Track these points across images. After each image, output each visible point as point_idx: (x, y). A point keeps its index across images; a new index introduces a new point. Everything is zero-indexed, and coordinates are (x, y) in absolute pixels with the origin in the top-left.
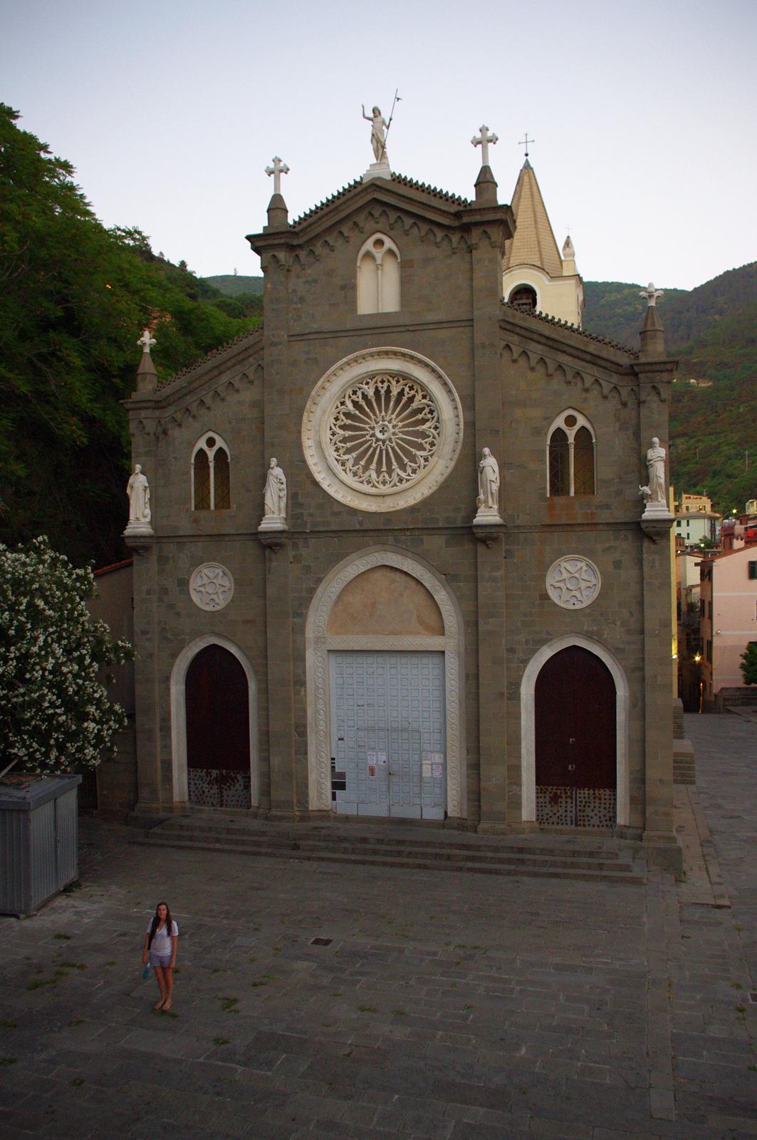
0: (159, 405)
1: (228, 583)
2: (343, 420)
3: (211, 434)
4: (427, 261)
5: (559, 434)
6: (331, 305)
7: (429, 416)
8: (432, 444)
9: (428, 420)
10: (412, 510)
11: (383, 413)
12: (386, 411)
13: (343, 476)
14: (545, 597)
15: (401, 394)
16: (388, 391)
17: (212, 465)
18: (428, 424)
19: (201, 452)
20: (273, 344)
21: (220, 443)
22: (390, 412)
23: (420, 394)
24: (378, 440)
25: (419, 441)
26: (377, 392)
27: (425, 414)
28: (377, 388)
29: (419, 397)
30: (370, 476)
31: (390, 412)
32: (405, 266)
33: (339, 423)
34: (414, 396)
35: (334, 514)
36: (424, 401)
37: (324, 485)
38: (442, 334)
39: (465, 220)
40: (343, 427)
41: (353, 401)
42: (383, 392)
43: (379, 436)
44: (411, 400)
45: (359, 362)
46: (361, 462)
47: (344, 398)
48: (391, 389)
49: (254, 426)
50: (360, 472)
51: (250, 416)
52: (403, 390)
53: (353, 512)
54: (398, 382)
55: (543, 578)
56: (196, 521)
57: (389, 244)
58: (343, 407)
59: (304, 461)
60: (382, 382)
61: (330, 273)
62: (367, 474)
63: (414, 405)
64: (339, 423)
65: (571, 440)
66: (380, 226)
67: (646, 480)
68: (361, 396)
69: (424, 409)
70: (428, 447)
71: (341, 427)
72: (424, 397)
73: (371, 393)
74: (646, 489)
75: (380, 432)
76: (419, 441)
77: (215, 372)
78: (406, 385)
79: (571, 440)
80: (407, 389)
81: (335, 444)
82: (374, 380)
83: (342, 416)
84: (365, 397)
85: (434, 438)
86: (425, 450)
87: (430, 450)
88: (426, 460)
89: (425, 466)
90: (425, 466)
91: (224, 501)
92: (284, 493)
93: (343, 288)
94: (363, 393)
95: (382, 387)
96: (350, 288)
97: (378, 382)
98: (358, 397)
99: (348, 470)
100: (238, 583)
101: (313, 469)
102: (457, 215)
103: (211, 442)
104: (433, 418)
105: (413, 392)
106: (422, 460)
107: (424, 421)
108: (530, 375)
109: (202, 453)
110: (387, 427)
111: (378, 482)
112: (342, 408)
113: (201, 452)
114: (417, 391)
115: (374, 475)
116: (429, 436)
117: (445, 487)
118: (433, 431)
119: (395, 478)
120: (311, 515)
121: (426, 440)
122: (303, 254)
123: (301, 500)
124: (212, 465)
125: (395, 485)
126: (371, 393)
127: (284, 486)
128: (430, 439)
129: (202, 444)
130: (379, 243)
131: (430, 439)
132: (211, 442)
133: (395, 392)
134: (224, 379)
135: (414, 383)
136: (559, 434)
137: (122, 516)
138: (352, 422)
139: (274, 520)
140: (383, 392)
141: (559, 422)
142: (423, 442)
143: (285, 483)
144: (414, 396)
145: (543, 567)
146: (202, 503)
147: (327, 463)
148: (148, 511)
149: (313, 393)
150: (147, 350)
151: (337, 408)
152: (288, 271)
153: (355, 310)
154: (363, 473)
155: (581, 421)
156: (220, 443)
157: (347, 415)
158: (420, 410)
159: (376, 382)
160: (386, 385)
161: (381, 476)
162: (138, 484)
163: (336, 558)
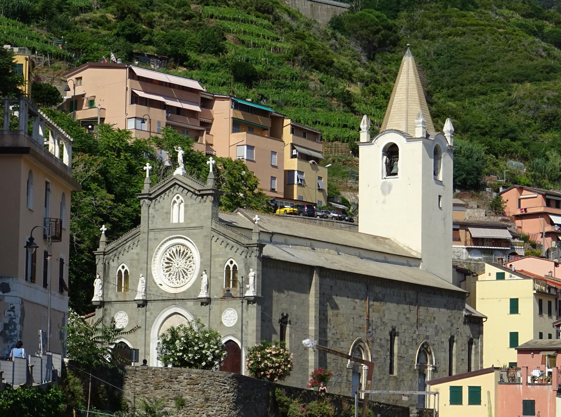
0: (104, 254)
1: (127, 318)
3: (123, 264)
4: (192, 204)
5: (228, 266)
6: (163, 219)
14: (221, 323)
15: (184, 251)
16: (180, 250)
17: (123, 275)
19: (120, 270)
20: (144, 233)
21: (126, 268)
26: (177, 250)
29: (189, 252)
32: (186, 206)
35: (162, 294)
38: (196, 231)
39: (201, 192)
43: (177, 266)
44: (187, 254)
53: (166, 293)
55: (221, 317)
56: (117, 296)
57: (181, 198)
61: (162, 208)
65: (231, 269)
66: (178, 192)
67: (248, 284)
74: (248, 286)
77: (125, 242)
79: (231, 269)
83: (166, 259)
84: (173, 252)
91: (127, 289)
93: (166, 213)
96: (168, 213)
100: (130, 318)
101: (154, 278)
102: (199, 191)
103: (123, 267)
108: (220, 246)
109: (120, 272)
110: (179, 263)
113: (120, 270)
117: (194, 285)
122: (154, 201)
124: (123, 275)
129: (120, 268)
130: (178, 198)
132: (123, 267)
133: (182, 251)
134: (128, 244)
136: (228, 267)
137: (92, 294)
139: (139, 296)
141: (228, 263)
145: (221, 312)
146: (120, 289)
148: (101, 292)
150: (103, 232)
152: (149, 206)
155: (235, 263)
156: (126, 268)
157: (168, 259)
158: (189, 257)
162: (97, 283)
163: (162, 309)
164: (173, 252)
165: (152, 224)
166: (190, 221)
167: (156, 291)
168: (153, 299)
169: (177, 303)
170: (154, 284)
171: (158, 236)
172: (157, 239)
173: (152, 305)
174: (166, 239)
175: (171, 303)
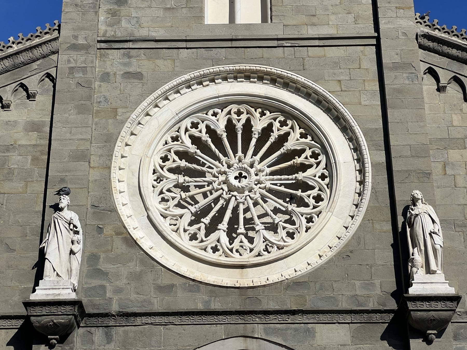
2: (174, 161)
6: (166, 9)
7: (313, 160)
8: (318, 199)
9: (310, 166)
10: (295, 284)
11: (240, 153)
12: (245, 151)
13: (173, 237)
18: (310, 172)
22: (250, 152)
23: (298, 131)
24: (231, 189)
25: (299, 193)
27: (306, 158)
28: (230, 121)
30: (218, 241)
31: (250, 152)
33: (169, 164)
34: (288, 134)
36: (303, 140)
37: (146, 244)
40: (175, 171)
41: (191, 137)
42: (239, 126)
43: (235, 183)
45: (205, 84)
46: (202, 220)
47: (178, 132)
48: (252, 123)
49: (30, 158)
50: (201, 235)
51: (23, 142)
52: (270, 126)
54: (262, 114)
58: (175, 143)
59: (114, 210)
60: (239, 113)
62: (213, 236)
63: (290, 145)
64: (169, 164)
68: (204, 130)
69: (303, 151)
70: (312, 202)
71: (171, 170)
72: (303, 136)
73: (220, 126)
75: (236, 178)
76: (299, 193)
78: (275, 119)
80: (276, 125)
81: (161, 193)
82: (226, 110)
83: (173, 156)
85: (320, 190)
86: (307, 205)
87: (315, 207)
88: (310, 220)
89: (308, 229)
90: (308, 229)
92: (77, 248)
94: (208, 127)
95: (239, 121)
97: (232, 112)
98: (200, 132)
99: (181, 230)
104: (318, 164)
105: (285, 129)
106: (304, 221)
107: (304, 168)
111: (231, 250)
112: (177, 146)
114: (292, 128)
115: (225, 240)
116: (312, 188)
117: (346, 254)
118: (320, 180)
119: (259, 245)
120: (118, 291)
121: (309, 192)
123: (103, 266)
125: (259, 255)
126: (220, 126)
127: (80, 237)
128: (314, 193)
131: (314, 193)
135: (289, 114)
138: (191, 160)
140: (239, 126)
142: (304, 194)
143: (81, 232)
144: (288, 134)
147: (149, 217)
149: (133, 116)
151: (166, 143)
153: (201, 18)
154: (207, 235)
159: (229, 113)
160: (244, 117)
161: (237, 242)
164: (211, 132)
165: (119, 22)
166: (304, 19)
167: (136, 277)
168: (115, 308)
169: (259, 330)
170: (120, 247)
171: (142, 63)
172: (138, 76)
173: (109, 338)
174: (187, 77)
175: (220, 330)
